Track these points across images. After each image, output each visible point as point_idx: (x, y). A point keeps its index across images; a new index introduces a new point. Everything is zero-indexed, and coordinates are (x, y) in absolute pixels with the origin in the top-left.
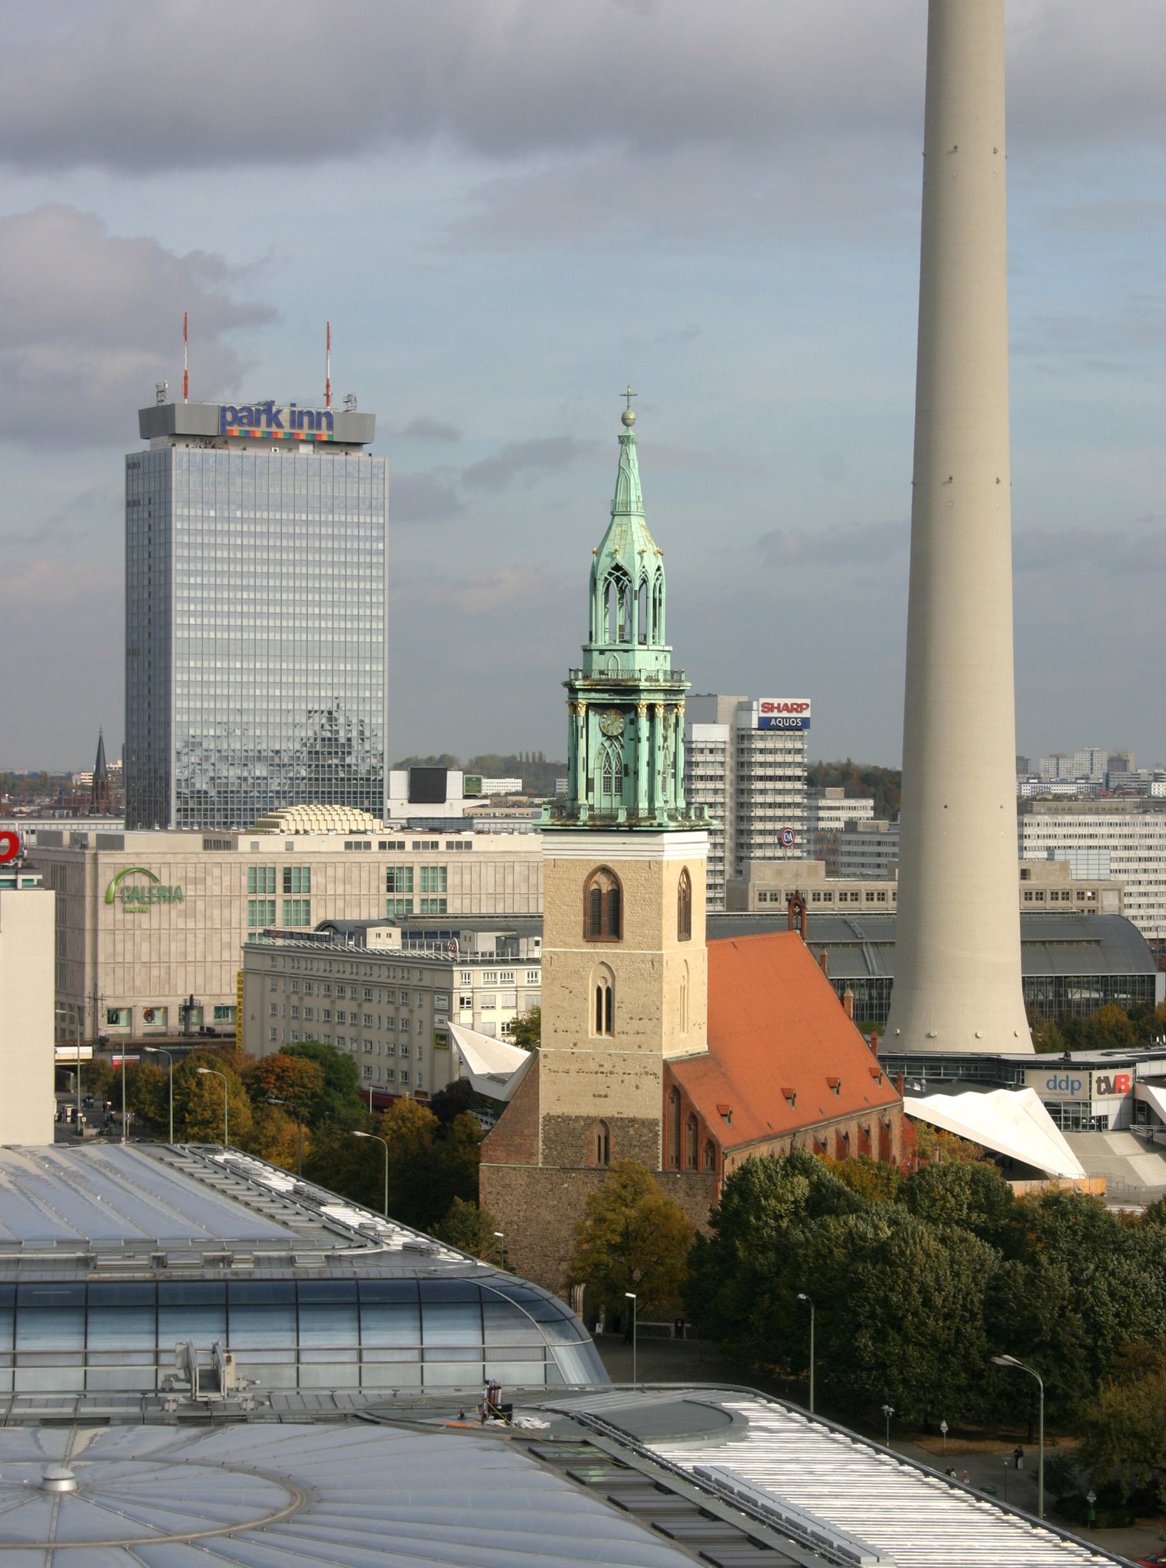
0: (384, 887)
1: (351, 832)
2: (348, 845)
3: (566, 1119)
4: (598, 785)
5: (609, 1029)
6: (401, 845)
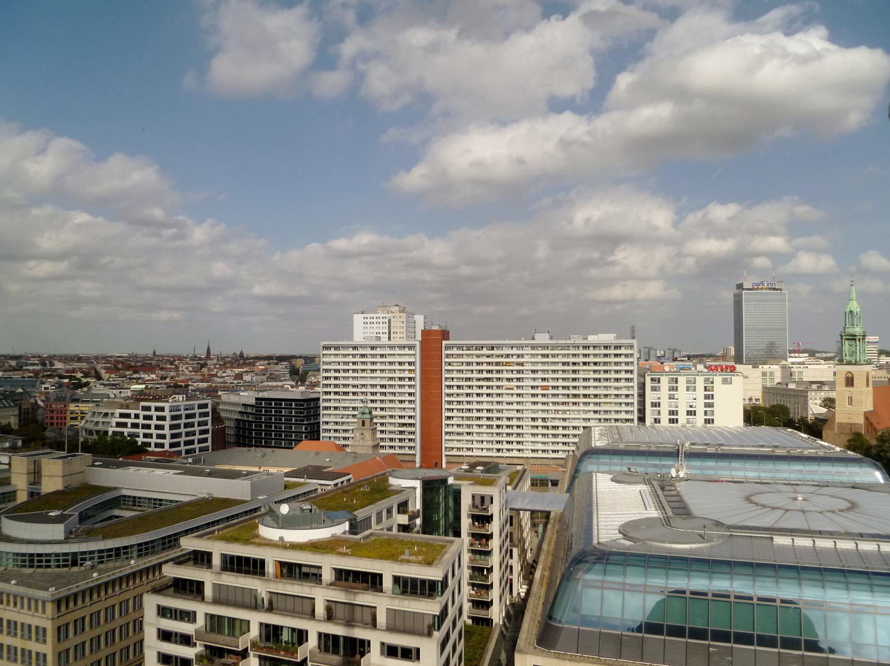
3: (842, 423)
4: (848, 355)
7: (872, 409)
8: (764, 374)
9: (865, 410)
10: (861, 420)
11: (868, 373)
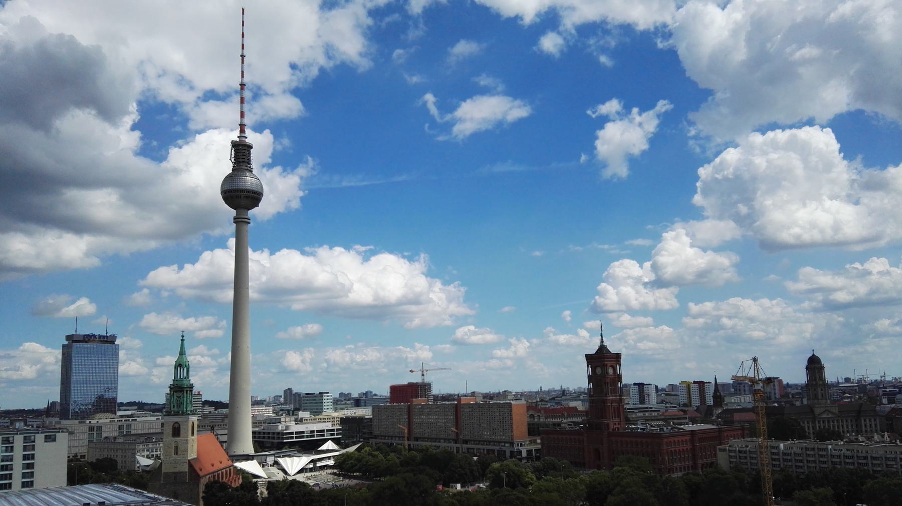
0: (118, 429)
1: (111, 418)
2: (110, 421)
4: (175, 407)
5: (177, 454)
6: (122, 420)
7: (196, 457)
8: (91, 429)
9: (189, 458)
10: (185, 468)
11: (193, 422)
